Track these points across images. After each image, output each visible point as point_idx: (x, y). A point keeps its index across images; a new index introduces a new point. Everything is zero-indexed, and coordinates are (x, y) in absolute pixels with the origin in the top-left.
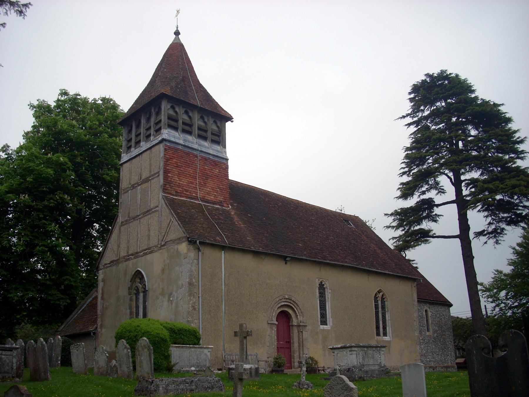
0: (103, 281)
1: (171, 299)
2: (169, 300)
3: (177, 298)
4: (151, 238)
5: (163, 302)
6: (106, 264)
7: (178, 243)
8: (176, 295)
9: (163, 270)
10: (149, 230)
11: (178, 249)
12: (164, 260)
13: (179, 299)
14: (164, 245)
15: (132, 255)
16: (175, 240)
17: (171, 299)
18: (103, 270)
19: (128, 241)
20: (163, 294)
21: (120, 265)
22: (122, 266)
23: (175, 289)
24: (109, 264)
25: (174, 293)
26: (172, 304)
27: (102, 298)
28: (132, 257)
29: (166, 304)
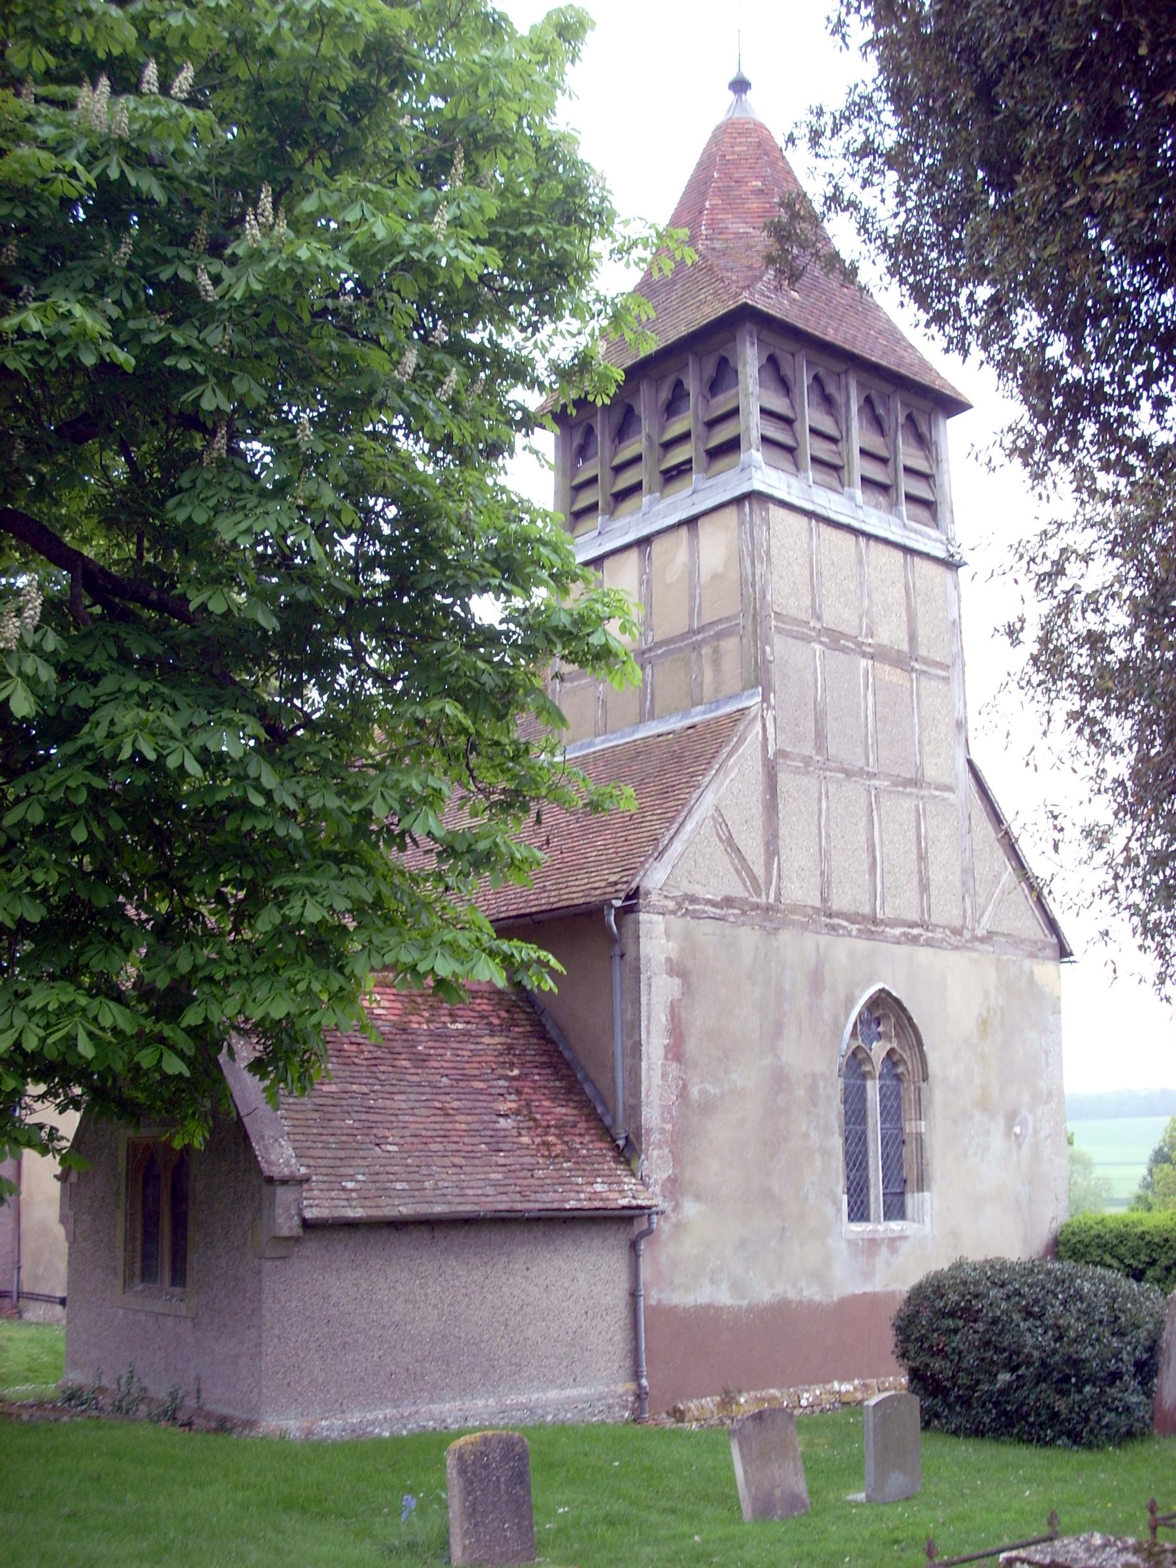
0: (676, 969)
1: (1017, 1130)
2: (1009, 1132)
3: (1036, 1131)
4: (934, 892)
5: (988, 1132)
6: (693, 900)
7: (1032, 955)
8: (1030, 1118)
9: (984, 1025)
10: (922, 858)
11: (1032, 973)
12: (986, 993)
13: (1043, 1134)
14: (982, 940)
15: (852, 918)
16: (1023, 941)
17: (1017, 1130)
18: (677, 923)
19: (824, 855)
20: (983, 1104)
21: (785, 935)
22: (796, 947)
23: (1026, 1098)
24: (714, 904)
25: (1024, 1112)
26: (1019, 1146)
27: (676, 1052)
28: (854, 928)
29: (998, 1142)
